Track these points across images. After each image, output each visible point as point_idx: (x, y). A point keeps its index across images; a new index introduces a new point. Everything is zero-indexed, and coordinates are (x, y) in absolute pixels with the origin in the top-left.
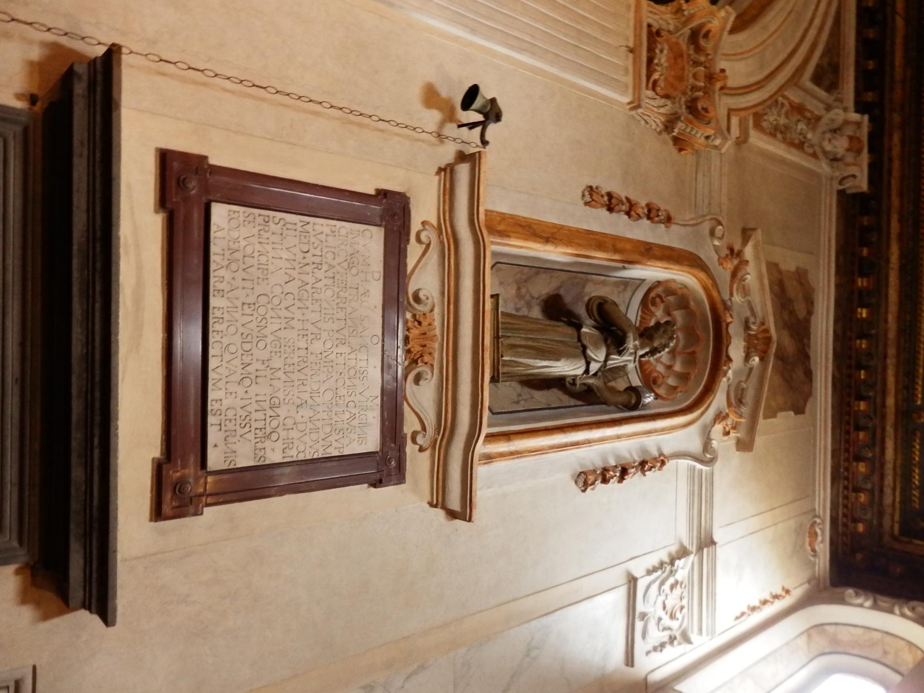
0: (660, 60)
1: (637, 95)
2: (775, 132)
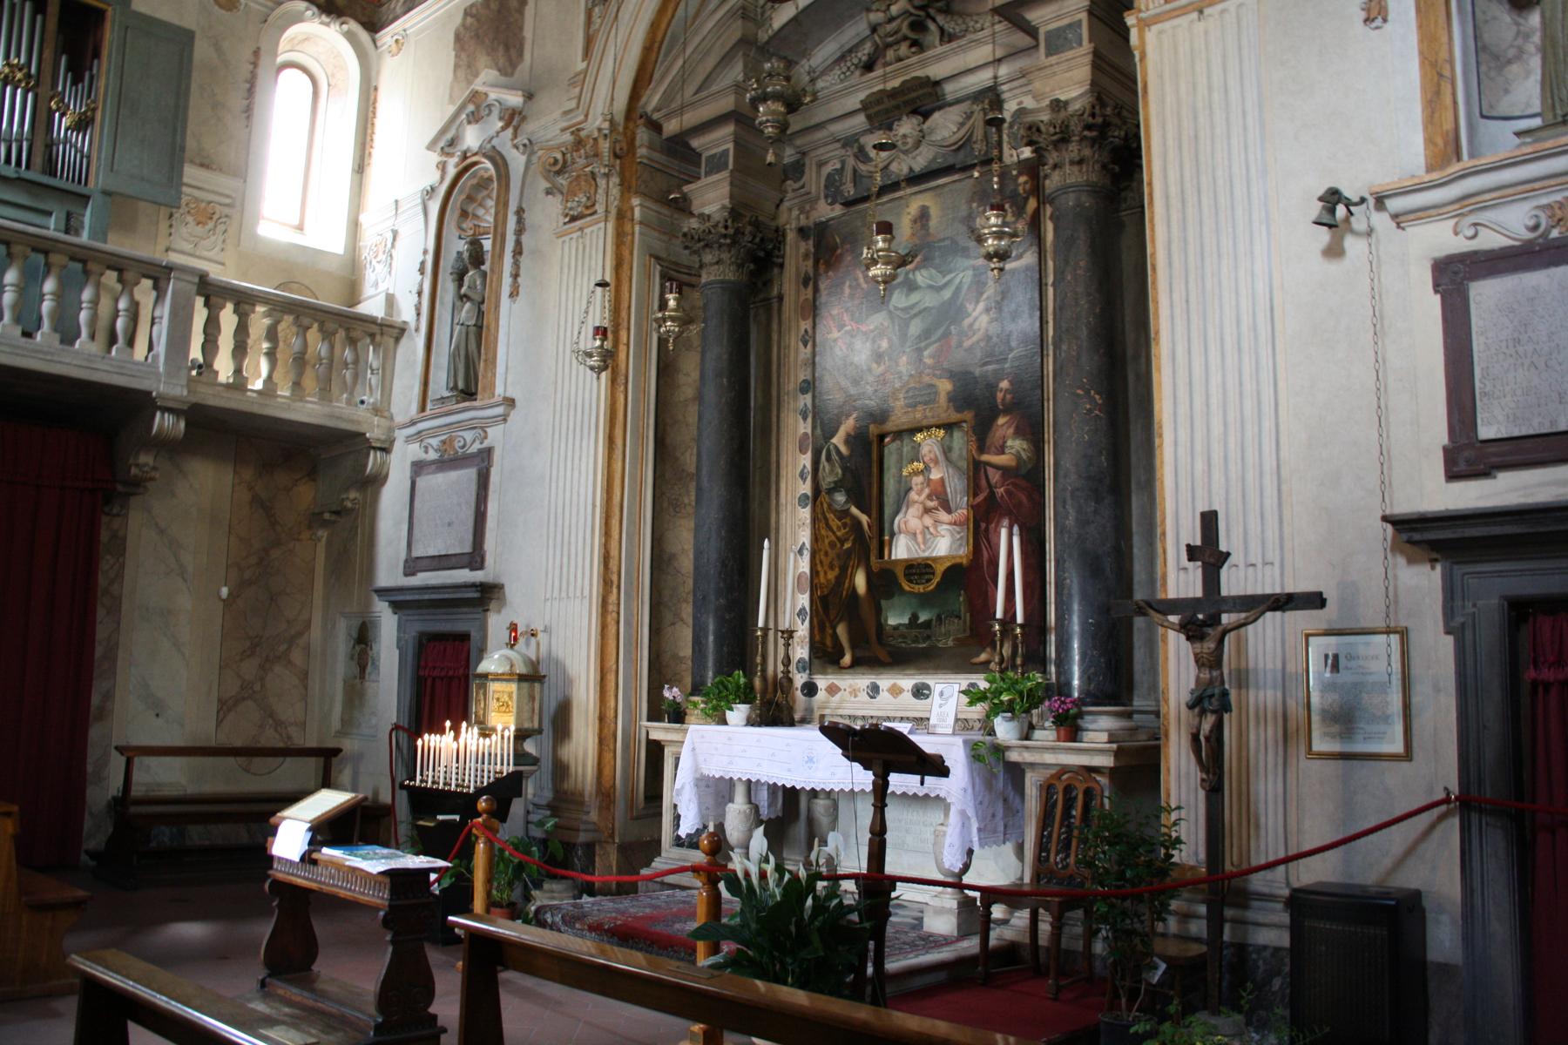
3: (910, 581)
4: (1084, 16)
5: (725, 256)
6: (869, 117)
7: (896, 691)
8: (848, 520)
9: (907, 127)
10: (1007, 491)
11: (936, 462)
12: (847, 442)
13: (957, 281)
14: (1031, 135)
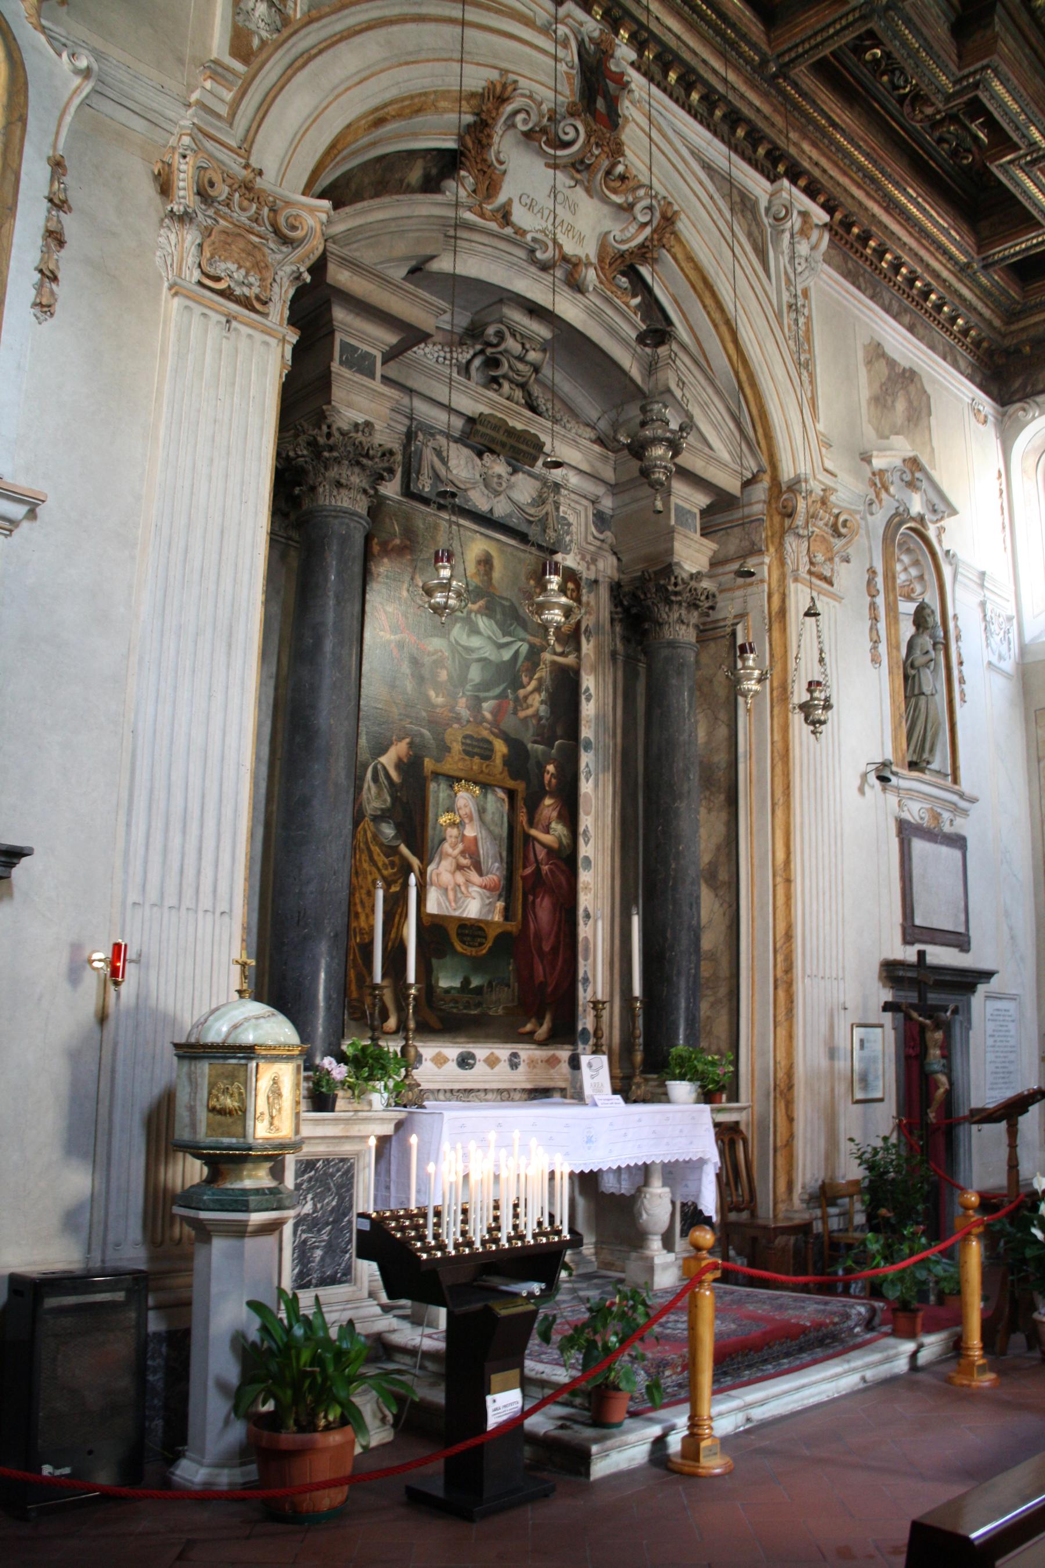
3: (463, 942)
7: (492, 1062)
8: (396, 859)
9: (499, 467)
10: (550, 870)
11: (471, 819)
12: (399, 765)
13: (515, 647)
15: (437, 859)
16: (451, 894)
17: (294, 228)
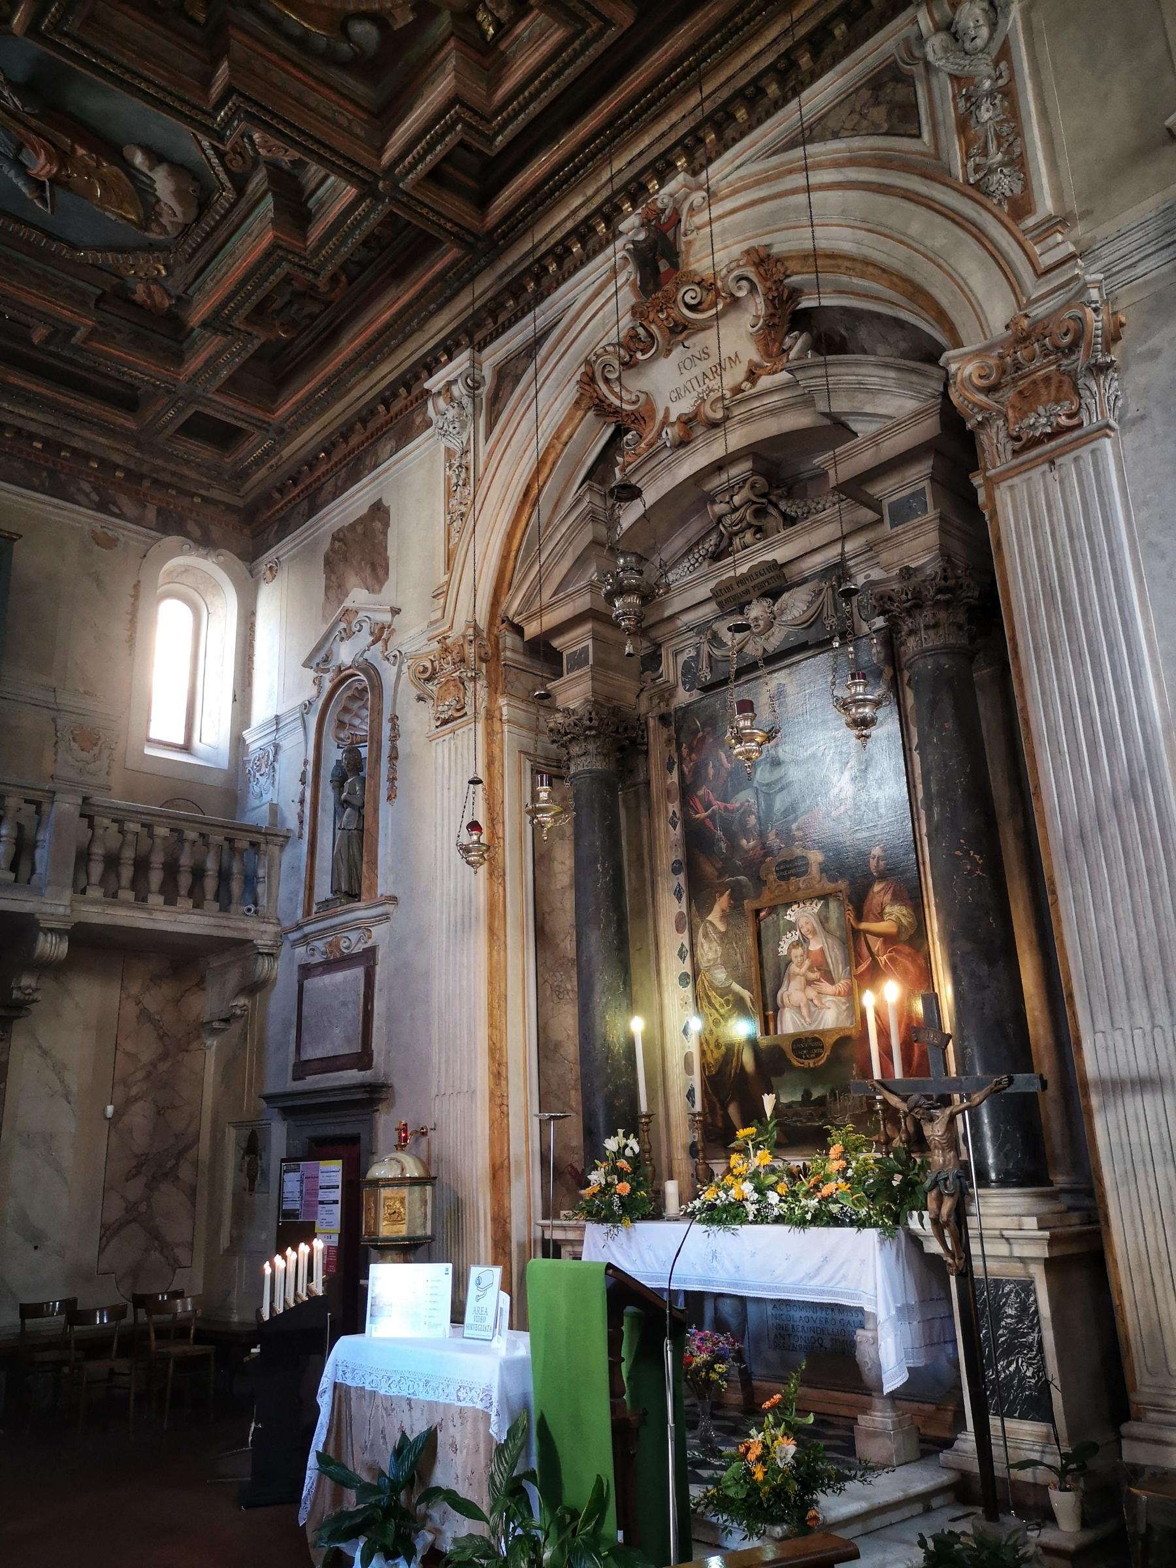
0: (1044, 425)
1: (1096, 435)
2: (1019, 163)
4: (926, 484)
5: (591, 747)
6: (720, 604)
8: (730, 997)
11: (814, 933)
12: (724, 917)
14: (883, 603)
15: (786, 983)
16: (804, 1011)
17: (425, 669)
